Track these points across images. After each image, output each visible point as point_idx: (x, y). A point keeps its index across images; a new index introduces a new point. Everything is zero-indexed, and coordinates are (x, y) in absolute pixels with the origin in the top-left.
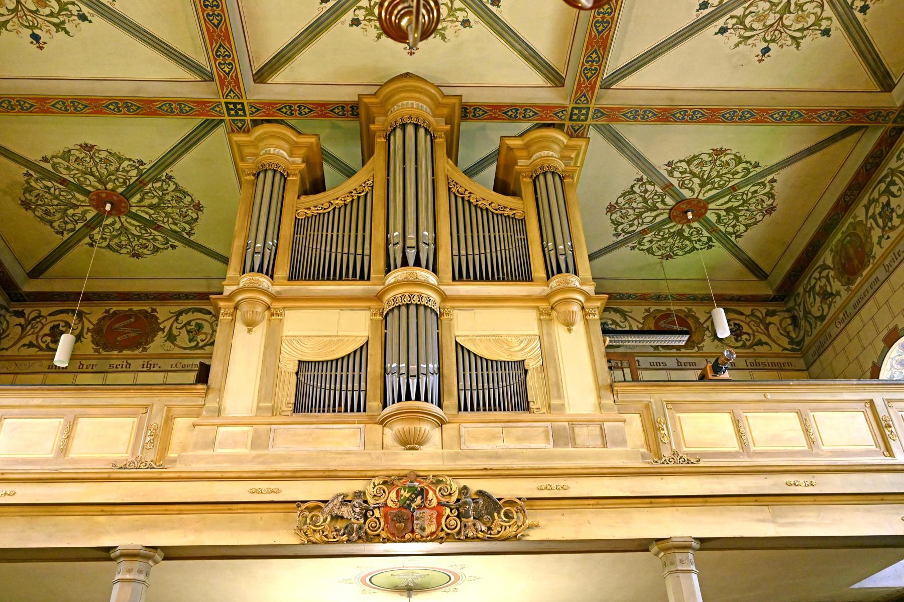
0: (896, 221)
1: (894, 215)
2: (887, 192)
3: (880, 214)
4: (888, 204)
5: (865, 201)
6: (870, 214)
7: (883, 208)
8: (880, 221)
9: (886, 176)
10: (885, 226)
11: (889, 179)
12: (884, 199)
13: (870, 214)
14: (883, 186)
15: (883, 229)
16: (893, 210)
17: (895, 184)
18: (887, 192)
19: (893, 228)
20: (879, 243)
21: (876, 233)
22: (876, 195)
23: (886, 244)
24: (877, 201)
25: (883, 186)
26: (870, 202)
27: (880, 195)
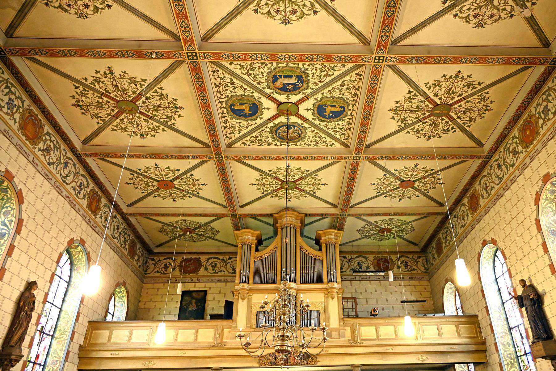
0: (551, 116)
1: (550, 112)
2: (547, 100)
3: (542, 112)
4: (547, 105)
5: (535, 105)
6: (537, 111)
7: (544, 109)
8: (543, 116)
9: (546, 91)
10: (545, 118)
11: (547, 93)
12: (545, 104)
13: (537, 111)
14: (544, 97)
15: (544, 120)
16: (549, 110)
17: (550, 95)
18: (547, 100)
19: (549, 120)
20: (542, 127)
21: (541, 121)
22: (540, 102)
23: (545, 128)
24: (541, 105)
25: (544, 97)
26: (537, 105)
27: (543, 102)
